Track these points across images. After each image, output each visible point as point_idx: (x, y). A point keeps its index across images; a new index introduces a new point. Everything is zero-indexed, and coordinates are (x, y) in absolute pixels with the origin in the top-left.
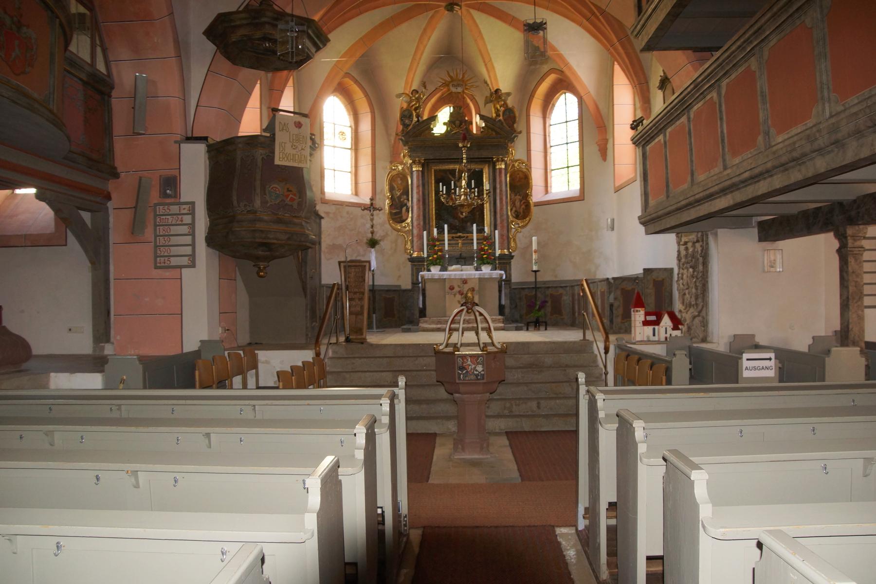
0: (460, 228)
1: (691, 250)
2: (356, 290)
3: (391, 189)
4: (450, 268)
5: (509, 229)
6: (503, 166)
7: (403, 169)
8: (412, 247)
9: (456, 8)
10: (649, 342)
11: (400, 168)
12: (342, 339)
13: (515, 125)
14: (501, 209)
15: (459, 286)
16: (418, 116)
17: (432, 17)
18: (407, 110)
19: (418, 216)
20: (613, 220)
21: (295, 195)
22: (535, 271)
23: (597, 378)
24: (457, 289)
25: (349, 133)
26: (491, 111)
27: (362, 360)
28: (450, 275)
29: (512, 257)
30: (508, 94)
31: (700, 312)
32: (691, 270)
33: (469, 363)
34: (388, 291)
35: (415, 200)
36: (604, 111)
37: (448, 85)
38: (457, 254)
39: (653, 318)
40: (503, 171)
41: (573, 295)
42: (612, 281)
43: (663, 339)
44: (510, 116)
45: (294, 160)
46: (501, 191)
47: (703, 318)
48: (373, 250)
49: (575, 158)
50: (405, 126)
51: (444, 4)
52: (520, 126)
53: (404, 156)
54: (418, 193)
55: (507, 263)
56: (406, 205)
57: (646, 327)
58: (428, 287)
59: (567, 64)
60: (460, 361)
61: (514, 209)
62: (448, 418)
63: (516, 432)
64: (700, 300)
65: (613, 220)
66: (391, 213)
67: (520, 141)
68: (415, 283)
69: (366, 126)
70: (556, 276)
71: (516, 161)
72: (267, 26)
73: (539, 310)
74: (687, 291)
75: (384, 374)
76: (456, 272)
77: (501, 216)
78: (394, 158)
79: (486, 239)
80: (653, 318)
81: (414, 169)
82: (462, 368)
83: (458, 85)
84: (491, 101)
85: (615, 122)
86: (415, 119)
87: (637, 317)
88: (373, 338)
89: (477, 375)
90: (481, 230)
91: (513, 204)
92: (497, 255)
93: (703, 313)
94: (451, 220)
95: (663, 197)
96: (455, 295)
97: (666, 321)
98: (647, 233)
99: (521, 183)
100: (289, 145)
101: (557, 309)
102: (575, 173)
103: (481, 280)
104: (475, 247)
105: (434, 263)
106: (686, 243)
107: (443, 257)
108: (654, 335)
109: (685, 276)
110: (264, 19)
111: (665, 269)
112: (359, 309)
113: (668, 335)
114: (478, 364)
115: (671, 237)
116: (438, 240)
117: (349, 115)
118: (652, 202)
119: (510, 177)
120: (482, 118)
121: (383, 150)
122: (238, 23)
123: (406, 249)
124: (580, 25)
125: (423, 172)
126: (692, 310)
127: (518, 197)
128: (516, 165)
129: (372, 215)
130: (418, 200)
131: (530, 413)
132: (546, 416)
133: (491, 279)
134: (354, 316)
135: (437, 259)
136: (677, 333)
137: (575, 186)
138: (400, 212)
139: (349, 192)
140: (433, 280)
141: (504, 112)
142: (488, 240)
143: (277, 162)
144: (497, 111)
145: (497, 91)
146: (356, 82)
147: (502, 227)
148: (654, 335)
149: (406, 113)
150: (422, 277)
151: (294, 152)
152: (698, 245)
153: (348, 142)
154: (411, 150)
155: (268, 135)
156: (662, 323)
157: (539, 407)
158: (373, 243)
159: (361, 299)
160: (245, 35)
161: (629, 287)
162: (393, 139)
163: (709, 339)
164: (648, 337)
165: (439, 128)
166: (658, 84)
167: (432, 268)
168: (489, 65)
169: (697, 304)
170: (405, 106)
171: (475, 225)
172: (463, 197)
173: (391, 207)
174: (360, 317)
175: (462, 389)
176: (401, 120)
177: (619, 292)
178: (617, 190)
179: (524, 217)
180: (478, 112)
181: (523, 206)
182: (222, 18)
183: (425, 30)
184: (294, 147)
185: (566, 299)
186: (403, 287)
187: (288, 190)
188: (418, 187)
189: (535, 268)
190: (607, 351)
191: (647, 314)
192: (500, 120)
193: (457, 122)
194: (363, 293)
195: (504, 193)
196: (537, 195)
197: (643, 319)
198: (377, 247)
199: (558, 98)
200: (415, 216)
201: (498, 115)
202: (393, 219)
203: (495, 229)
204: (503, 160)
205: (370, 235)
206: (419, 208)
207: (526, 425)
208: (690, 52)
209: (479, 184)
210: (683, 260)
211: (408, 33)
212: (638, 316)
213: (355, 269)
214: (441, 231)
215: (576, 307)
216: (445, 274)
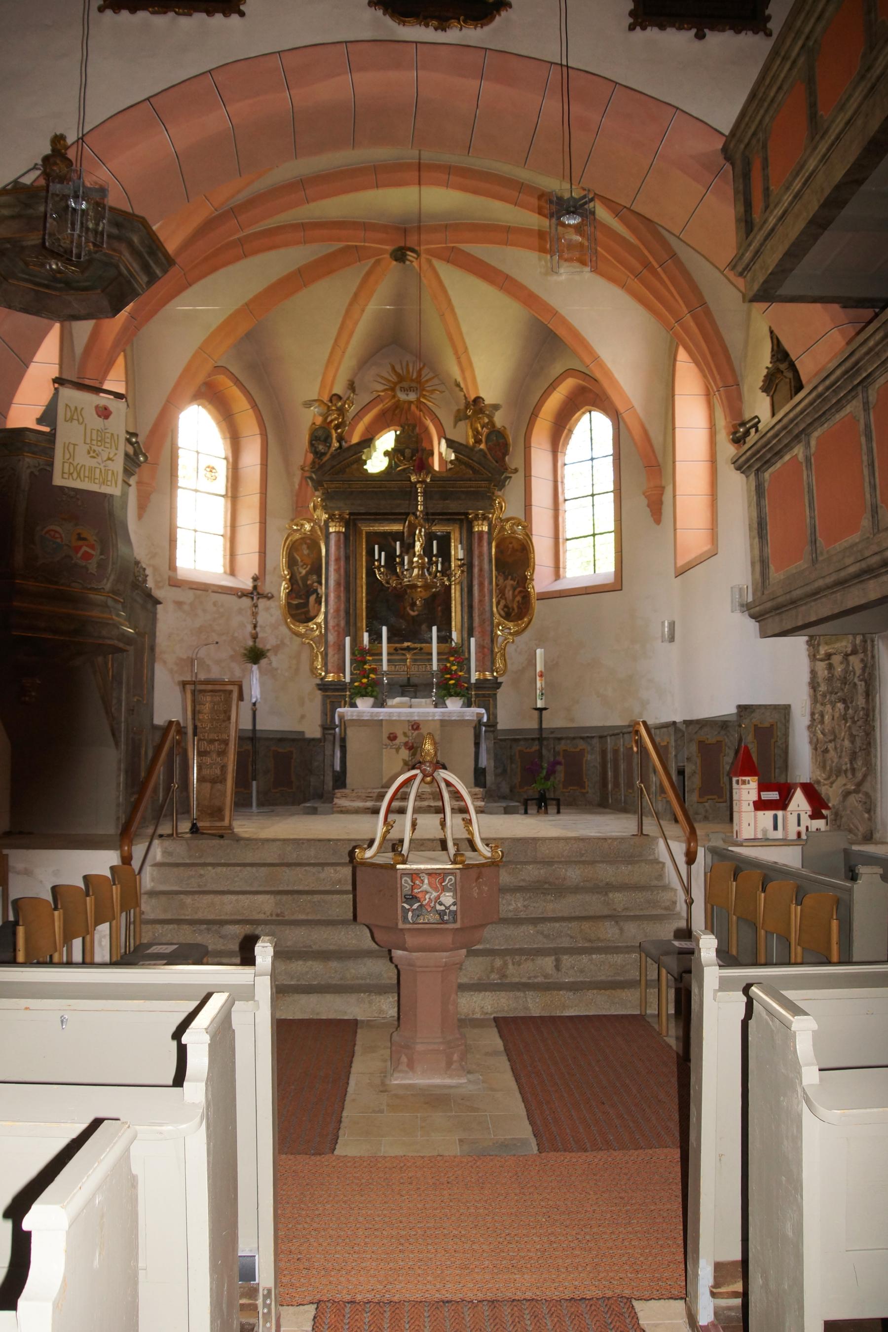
0: (408, 633)
1: (839, 670)
2: (212, 736)
3: (291, 563)
4: (390, 702)
5: (493, 638)
6: (485, 529)
7: (313, 529)
8: (325, 664)
10: (765, 842)
11: (307, 527)
12: (185, 827)
13: (507, 458)
14: (481, 601)
15: (405, 734)
16: (340, 439)
17: (369, 274)
18: (321, 427)
19: (337, 611)
20: (672, 625)
21: (92, 547)
22: (541, 710)
23: (666, 909)
24: (401, 739)
25: (222, 469)
26: (464, 434)
27: (219, 869)
28: (390, 714)
29: (498, 685)
30: (496, 407)
31: (859, 784)
32: (840, 706)
33: (426, 886)
34: (281, 740)
35: (332, 583)
36: (657, 438)
37: (393, 389)
38: (403, 678)
39: (774, 795)
40: (485, 537)
41: (604, 753)
42: (683, 727)
43: (793, 836)
44: (499, 443)
45: (92, 479)
46: (481, 570)
47: (867, 795)
48: (255, 667)
49: (606, 518)
50: (318, 454)
51: (389, 248)
52: (514, 460)
53: (315, 508)
54: (337, 571)
55: (489, 696)
56: (316, 591)
57: (760, 813)
58: (350, 732)
59: (596, 358)
60: (406, 882)
61: (503, 603)
62: (381, 990)
63: (515, 1019)
64: (860, 763)
65: (672, 625)
66: (289, 604)
67: (515, 484)
68: (328, 727)
69: (251, 458)
70: (572, 720)
71: (508, 520)
73: (547, 778)
74: (831, 746)
75: (260, 898)
76: (400, 709)
77: (481, 614)
78: (299, 510)
79: (454, 652)
80: (774, 795)
81: (331, 530)
82: (412, 898)
83: (411, 389)
84: (467, 417)
85: (678, 457)
86: (336, 444)
87: (744, 793)
88: (246, 826)
89: (441, 914)
90: (445, 639)
91: (502, 593)
92: (473, 681)
93: (866, 787)
94: (393, 620)
95: (803, 564)
96: (398, 750)
97: (799, 802)
98: (764, 634)
99: (515, 558)
100: (82, 449)
101: (575, 777)
102: (607, 547)
103: (444, 723)
104: (435, 667)
105: (363, 692)
106: (829, 656)
107: (377, 683)
108: (775, 828)
109: (827, 718)
111: (775, 708)
112: (218, 772)
113: (803, 829)
114: (444, 889)
115: (799, 643)
116: (370, 652)
117: (224, 438)
118: (776, 575)
119: (497, 547)
120: (451, 444)
121: (280, 501)
123: (313, 670)
124: (623, 286)
125: (346, 535)
126: (841, 780)
127: (510, 582)
128: (507, 527)
129: (256, 606)
130: (338, 584)
131: (540, 979)
132: (574, 987)
133: (461, 723)
134: (208, 785)
135: (366, 686)
136: (820, 824)
137: (607, 567)
138: (306, 604)
139: (221, 570)
140: (360, 723)
141: (488, 436)
142: (459, 655)
143: (58, 481)
144: (476, 434)
145: (478, 400)
146: (237, 382)
147: (483, 633)
148: (775, 828)
149: (320, 433)
150: (341, 718)
151: (93, 463)
152: (855, 662)
153: (221, 485)
154: (328, 497)
155: (46, 429)
156: (792, 806)
157: (557, 968)
158: (255, 655)
159: (222, 753)
161: (711, 737)
162: (297, 480)
163: (877, 836)
164: (765, 831)
165: (376, 463)
166: (761, 384)
167: (359, 702)
168: (463, 358)
169: (853, 770)
170: (319, 421)
171: (434, 629)
172: (416, 571)
173: (289, 595)
174: (219, 786)
175: (410, 940)
176: (311, 444)
177: (694, 748)
178: (680, 572)
179: (520, 617)
180: (442, 435)
181: (518, 598)
183: (356, 296)
184: (92, 454)
185: (592, 759)
186: (308, 735)
187: (80, 538)
188: (337, 560)
189: (540, 704)
190: (691, 858)
191: (762, 788)
192: (481, 450)
193: (408, 452)
194: (226, 742)
195: (486, 575)
196: (541, 580)
197: (755, 798)
198: (264, 662)
199: (578, 420)
200: (331, 611)
201: (478, 441)
202: (293, 616)
203: (471, 634)
204: (485, 518)
205: (250, 643)
206: (338, 597)
207: (535, 1005)
208: (836, 306)
209: (445, 553)
210: (823, 688)
211: (329, 296)
212: (747, 791)
213: (213, 695)
214: (376, 637)
215: (610, 774)
216: (382, 713)
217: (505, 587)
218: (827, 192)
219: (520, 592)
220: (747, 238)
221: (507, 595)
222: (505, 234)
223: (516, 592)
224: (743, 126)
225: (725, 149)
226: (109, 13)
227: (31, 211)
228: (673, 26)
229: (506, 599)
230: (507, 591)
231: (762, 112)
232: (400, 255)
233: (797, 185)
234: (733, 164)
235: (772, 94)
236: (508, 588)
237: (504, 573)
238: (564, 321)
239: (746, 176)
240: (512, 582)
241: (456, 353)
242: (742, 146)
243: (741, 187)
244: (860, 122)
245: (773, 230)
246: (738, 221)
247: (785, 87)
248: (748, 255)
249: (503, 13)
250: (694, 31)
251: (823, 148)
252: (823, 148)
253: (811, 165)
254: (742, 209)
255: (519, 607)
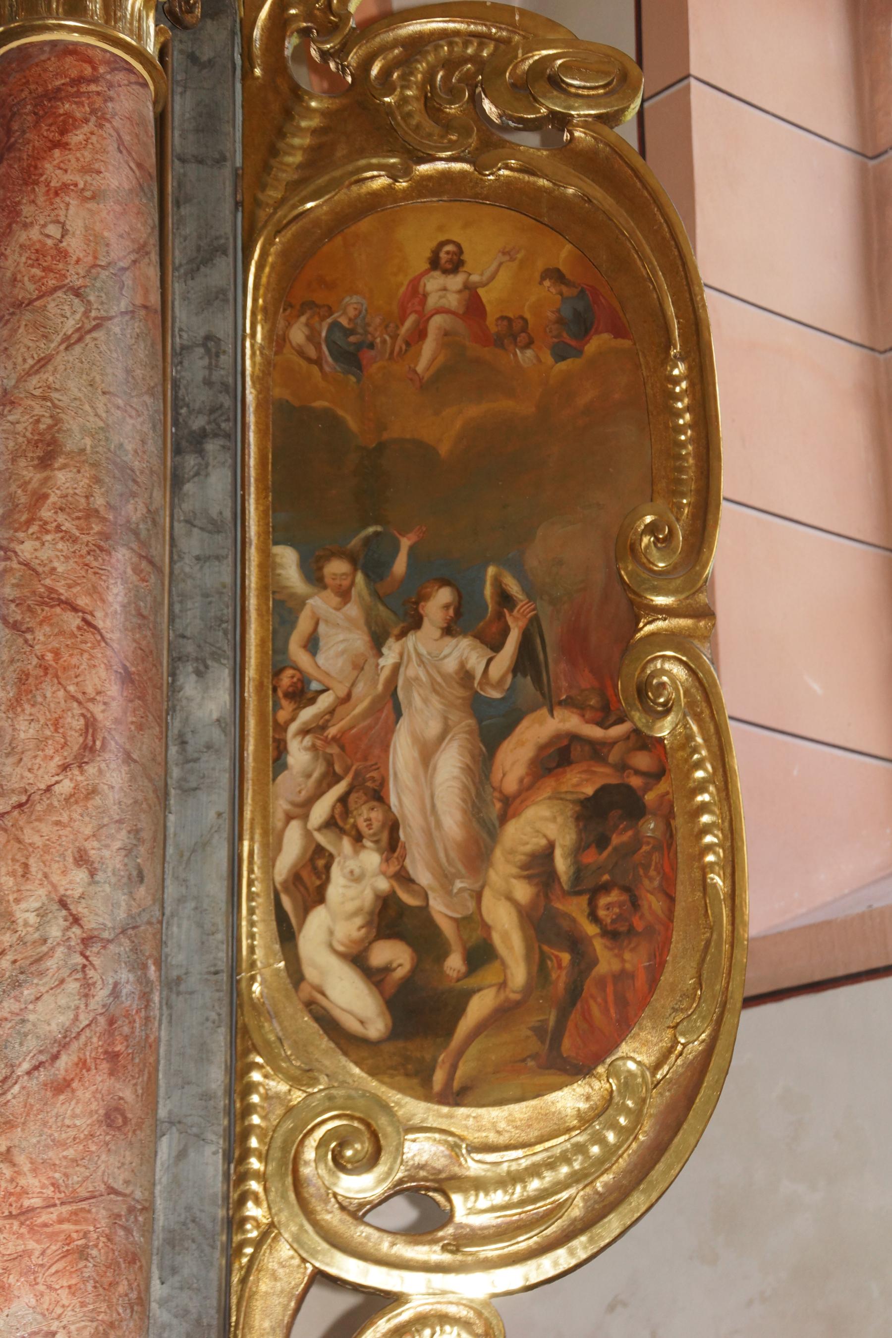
61: (356, 880)
181: (543, 824)
217: (391, 704)
219: (557, 756)
221: (403, 798)
223: (515, 758)
229: (392, 843)
230: (403, 752)
236: (423, 715)
237: (372, 563)
240: (464, 652)
255: (541, 925)
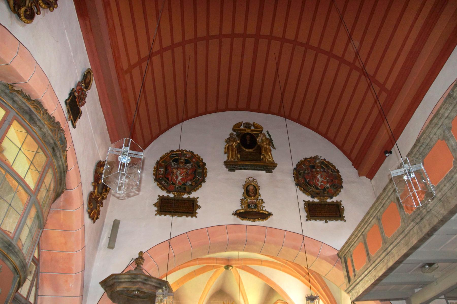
9: (230, 268)
17: (216, 271)
51: (224, 266)
72: (140, 284)
110: (139, 280)
122: (123, 280)
124: (299, 279)
160: (126, 288)
182: (113, 277)
183: (211, 278)
208: (378, 301)
218: (377, 278)
220: (349, 283)
222: (261, 262)
224: (343, 250)
225: (338, 254)
226: (158, 215)
227: (134, 280)
228: (319, 219)
231: (350, 247)
232: (227, 267)
233: (366, 273)
234: (341, 259)
235: (353, 243)
238: (278, 286)
239: (346, 263)
241: (243, 296)
242: (344, 255)
243: (345, 266)
244: (385, 261)
245: (358, 283)
246: (345, 276)
247: (357, 242)
248: (350, 288)
249: (271, 217)
250: (324, 221)
251: (374, 265)
252: (374, 265)
253: (370, 268)
254: (346, 273)
